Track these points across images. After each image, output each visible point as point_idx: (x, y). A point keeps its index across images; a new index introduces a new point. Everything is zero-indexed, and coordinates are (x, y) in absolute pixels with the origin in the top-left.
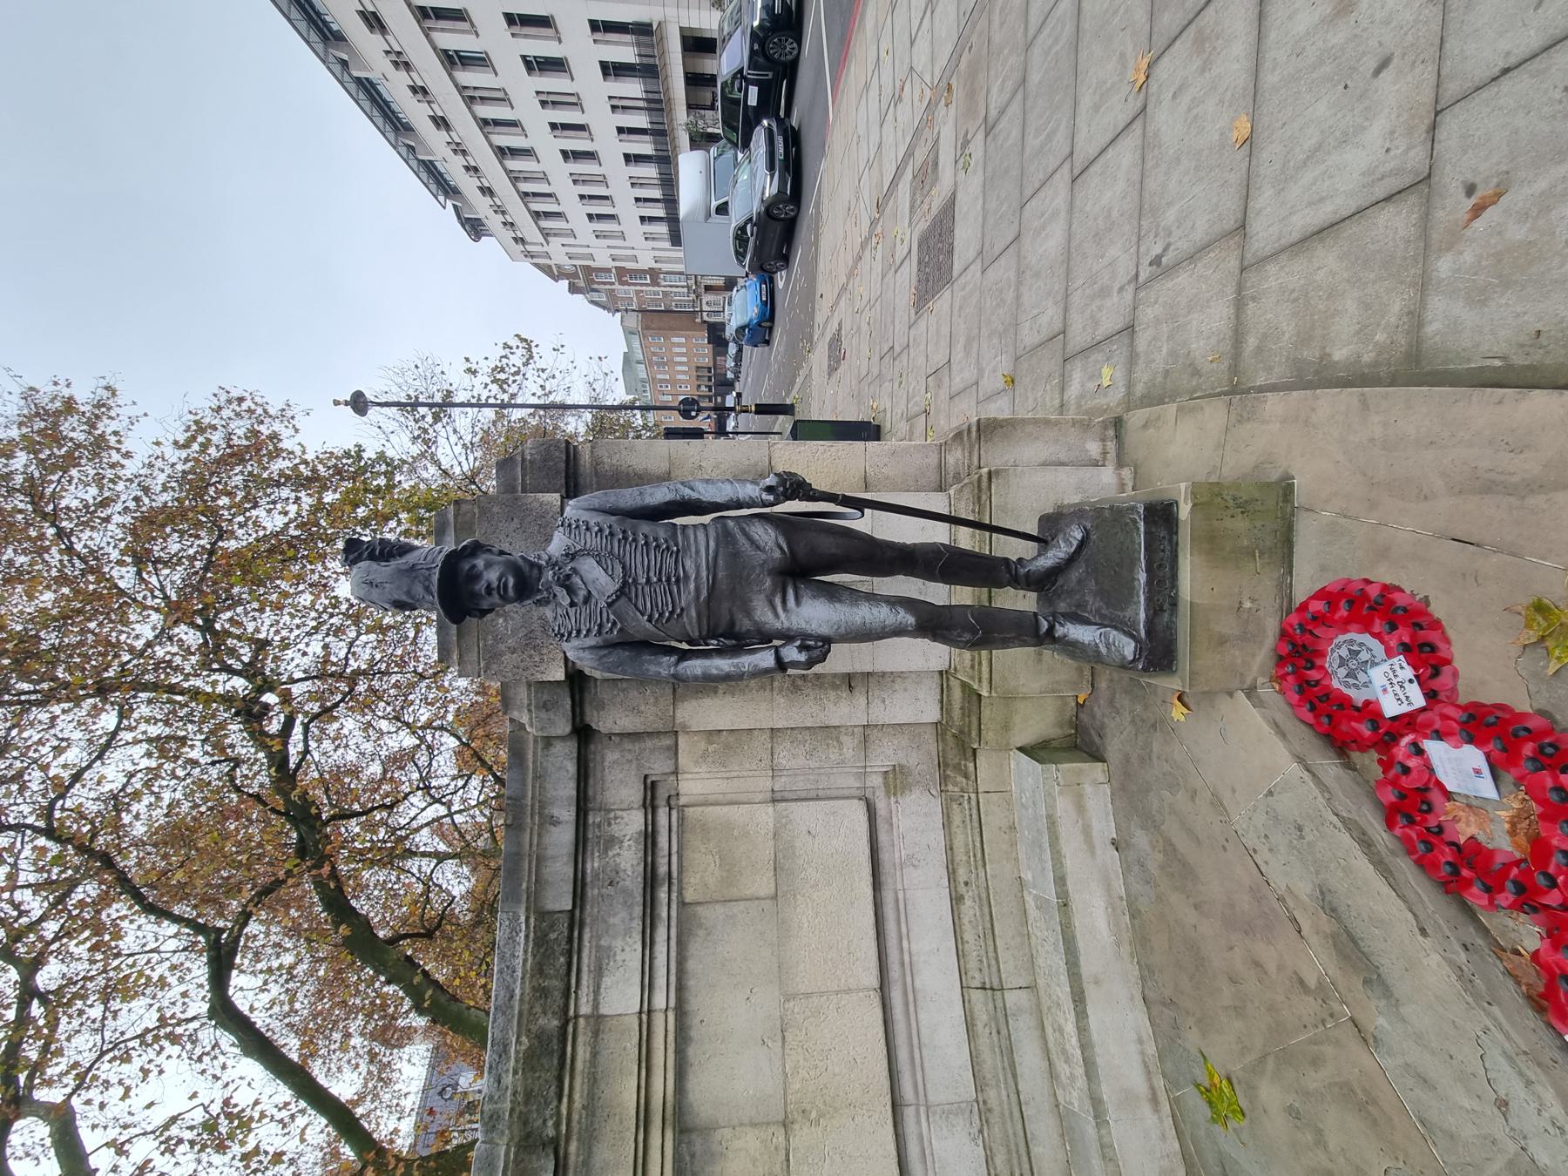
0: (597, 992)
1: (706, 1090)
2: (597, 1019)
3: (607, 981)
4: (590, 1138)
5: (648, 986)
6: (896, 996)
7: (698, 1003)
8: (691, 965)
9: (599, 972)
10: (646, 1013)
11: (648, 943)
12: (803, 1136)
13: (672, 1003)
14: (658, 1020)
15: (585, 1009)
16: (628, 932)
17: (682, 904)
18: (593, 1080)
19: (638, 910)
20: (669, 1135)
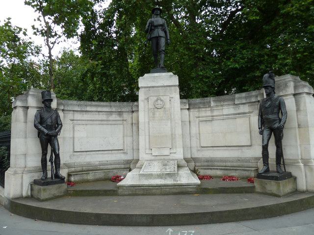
15: (224, 107)
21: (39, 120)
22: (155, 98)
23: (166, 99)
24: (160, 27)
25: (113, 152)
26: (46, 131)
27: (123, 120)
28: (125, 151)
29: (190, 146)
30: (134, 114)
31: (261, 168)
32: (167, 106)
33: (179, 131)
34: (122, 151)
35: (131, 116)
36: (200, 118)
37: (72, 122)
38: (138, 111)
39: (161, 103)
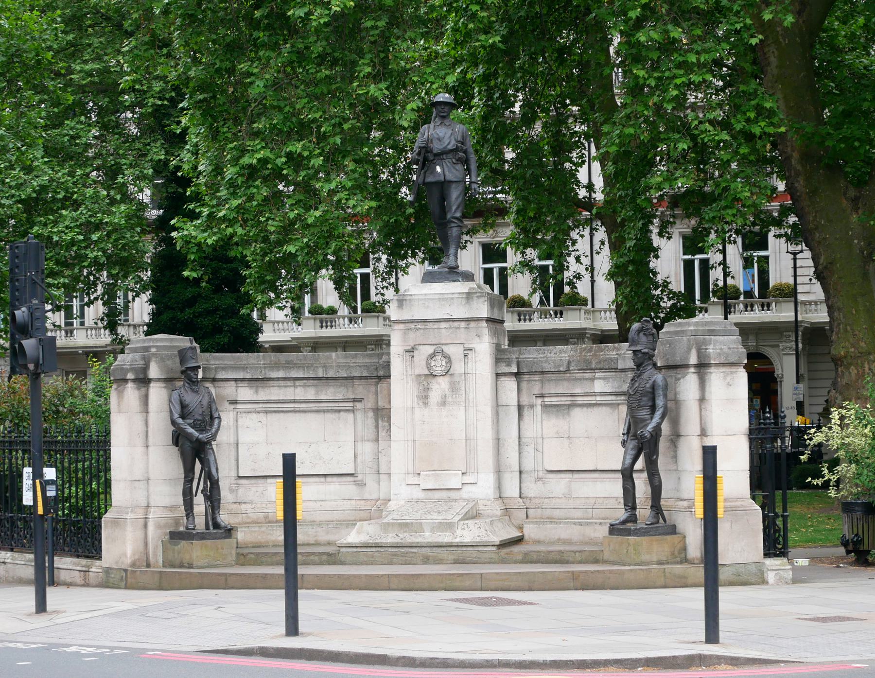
0: (600, 378)
1: (577, 412)
2: (593, 379)
3: (601, 381)
4: (568, 380)
5: (602, 394)
6: (596, 475)
7: (596, 410)
8: (604, 408)
9: (604, 379)
10: (594, 394)
11: (611, 394)
12: (566, 441)
13: (598, 402)
14: (593, 398)
15: (597, 375)
16: (613, 387)
17: (619, 404)
18: (580, 379)
19: (617, 390)
20: (569, 403)
22: (430, 350)
24: (450, 156)
25: (329, 479)
27: (354, 400)
28: (360, 477)
29: (517, 469)
30: (382, 385)
31: (621, 514)
32: (458, 367)
33: (485, 432)
34: (351, 479)
35: (373, 389)
36: (546, 399)
37: (233, 406)
38: (389, 377)
39: (444, 363)
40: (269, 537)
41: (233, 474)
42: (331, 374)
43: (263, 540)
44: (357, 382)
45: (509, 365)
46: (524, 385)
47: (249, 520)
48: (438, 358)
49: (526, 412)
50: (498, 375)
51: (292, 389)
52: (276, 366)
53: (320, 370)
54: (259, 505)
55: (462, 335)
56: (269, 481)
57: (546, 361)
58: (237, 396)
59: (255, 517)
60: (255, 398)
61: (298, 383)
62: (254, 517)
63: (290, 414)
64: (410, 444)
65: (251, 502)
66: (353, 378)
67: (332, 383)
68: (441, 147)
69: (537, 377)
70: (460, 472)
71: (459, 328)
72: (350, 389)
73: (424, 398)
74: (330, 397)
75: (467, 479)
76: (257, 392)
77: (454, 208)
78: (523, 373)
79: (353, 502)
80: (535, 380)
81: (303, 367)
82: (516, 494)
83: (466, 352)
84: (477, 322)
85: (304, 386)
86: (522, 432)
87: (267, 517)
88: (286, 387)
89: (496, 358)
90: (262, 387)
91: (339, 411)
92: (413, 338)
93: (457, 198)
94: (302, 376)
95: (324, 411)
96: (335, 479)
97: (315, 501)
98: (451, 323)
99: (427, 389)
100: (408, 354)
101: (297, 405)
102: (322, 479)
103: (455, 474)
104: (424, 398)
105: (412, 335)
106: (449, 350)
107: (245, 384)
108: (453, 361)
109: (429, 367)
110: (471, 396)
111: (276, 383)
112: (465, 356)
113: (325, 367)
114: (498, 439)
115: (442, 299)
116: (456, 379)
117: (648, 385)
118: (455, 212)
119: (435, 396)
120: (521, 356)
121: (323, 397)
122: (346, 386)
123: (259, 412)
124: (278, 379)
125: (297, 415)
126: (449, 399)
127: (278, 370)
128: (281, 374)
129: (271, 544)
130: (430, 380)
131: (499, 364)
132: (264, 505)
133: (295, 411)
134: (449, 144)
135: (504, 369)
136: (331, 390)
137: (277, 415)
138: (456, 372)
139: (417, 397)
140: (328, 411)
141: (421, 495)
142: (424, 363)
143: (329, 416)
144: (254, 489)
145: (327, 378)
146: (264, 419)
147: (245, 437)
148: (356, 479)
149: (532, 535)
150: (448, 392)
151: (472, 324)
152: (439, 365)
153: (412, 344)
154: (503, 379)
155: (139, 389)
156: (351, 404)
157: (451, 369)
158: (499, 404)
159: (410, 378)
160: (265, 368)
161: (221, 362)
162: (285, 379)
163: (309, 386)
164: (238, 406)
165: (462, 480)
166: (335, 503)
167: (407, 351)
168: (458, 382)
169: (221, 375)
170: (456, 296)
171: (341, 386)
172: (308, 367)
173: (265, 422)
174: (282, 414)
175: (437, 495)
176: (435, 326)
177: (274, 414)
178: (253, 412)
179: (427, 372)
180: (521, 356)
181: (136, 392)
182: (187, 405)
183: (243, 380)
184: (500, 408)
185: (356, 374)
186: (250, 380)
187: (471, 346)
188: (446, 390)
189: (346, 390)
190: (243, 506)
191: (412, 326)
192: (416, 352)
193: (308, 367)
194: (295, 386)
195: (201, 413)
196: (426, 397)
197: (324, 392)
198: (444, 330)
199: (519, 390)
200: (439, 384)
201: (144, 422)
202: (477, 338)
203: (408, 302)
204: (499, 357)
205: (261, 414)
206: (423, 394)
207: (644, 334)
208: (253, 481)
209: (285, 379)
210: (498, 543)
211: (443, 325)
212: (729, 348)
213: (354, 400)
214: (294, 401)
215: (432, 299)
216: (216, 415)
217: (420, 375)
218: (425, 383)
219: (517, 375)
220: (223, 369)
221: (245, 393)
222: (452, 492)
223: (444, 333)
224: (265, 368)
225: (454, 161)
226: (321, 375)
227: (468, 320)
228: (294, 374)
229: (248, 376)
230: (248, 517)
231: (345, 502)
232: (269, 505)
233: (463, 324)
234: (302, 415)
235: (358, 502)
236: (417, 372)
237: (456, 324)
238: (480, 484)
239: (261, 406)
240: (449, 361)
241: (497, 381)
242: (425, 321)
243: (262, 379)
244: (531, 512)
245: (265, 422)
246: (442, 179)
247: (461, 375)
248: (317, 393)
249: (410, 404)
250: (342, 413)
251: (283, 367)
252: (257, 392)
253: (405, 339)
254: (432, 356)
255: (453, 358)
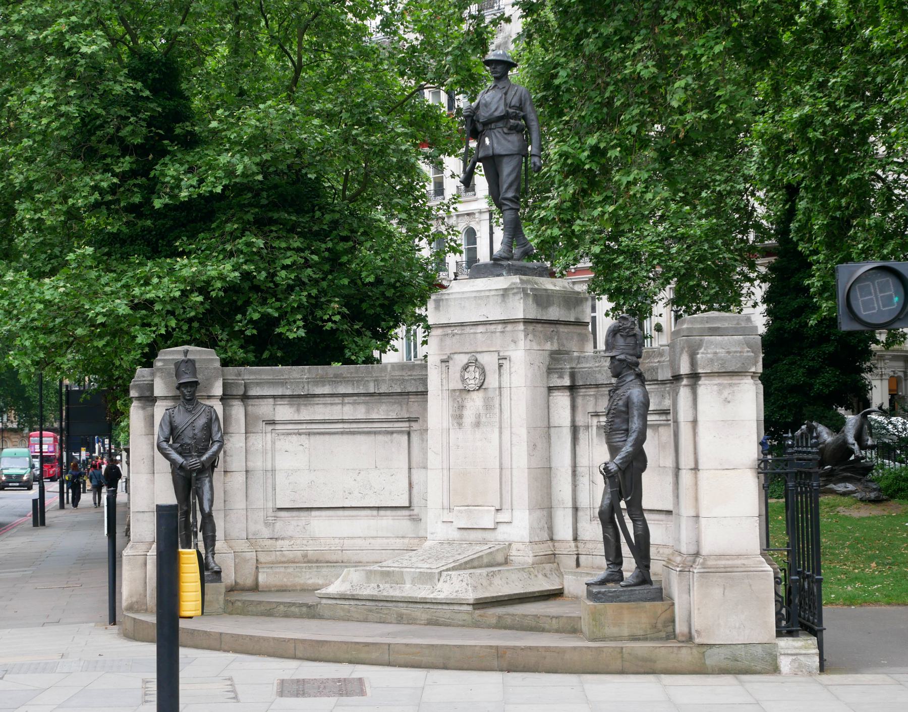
21: (167, 431)
22: (463, 359)
23: (489, 360)
24: (500, 124)
25: (382, 512)
26: (180, 459)
27: (410, 420)
28: (416, 511)
32: (492, 381)
34: (406, 513)
37: (270, 428)
39: (477, 376)
40: (297, 580)
41: (270, 505)
42: (384, 389)
43: (289, 584)
44: (412, 398)
45: (561, 377)
46: (579, 401)
47: (283, 559)
48: (471, 369)
49: (582, 436)
50: (550, 389)
51: (340, 407)
52: (322, 381)
53: (372, 385)
54: (298, 542)
55: (497, 342)
56: (314, 513)
57: (600, 372)
58: (274, 415)
59: (291, 556)
60: (296, 417)
61: (347, 400)
62: (290, 555)
63: (337, 437)
64: (445, 472)
65: (291, 537)
66: (408, 394)
67: (385, 399)
68: (487, 115)
69: (592, 392)
70: (493, 508)
71: (495, 332)
72: (404, 406)
73: (458, 418)
74: (382, 416)
75: (502, 517)
76: (298, 410)
77: (505, 186)
78: (579, 387)
79: (406, 541)
80: (589, 395)
81: (352, 381)
82: (569, 536)
83: (501, 361)
84: (514, 325)
85: (354, 403)
86: (578, 459)
87: (305, 556)
88: (332, 404)
89: (549, 369)
90: (305, 405)
91: (392, 433)
92: (452, 344)
93: (509, 175)
94: (351, 391)
95: (375, 433)
96: (389, 513)
97: (365, 538)
98: (488, 326)
99: (461, 407)
100: (444, 364)
101: (346, 426)
102: (375, 512)
103: (488, 510)
104: (458, 418)
105: (448, 341)
106: (484, 359)
107: (286, 401)
108: (488, 373)
109: (463, 380)
110: (506, 414)
111: (322, 400)
112: (500, 366)
113: (377, 381)
114: (550, 468)
115: (480, 297)
116: (490, 394)
117: (621, 403)
118: (506, 191)
119: (469, 415)
120: (579, 366)
121: (374, 416)
122: (400, 404)
123: (300, 434)
124: (324, 395)
125: (345, 437)
126: (483, 419)
127: (324, 386)
128: (326, 390)
129: (299, 588)
130: (464, 395)
131: (551, 376)
132: (305, 542)
133: (342, 433)
134: (496, 110)
135: (556, 381)
136: (384, 407)
137: (322, 437)
138: (491, 386)
139: (452, 416)
140: (380, 433)
141: (456, 535)
142: (458, 375)
143: (380, 438)
144: (294, 523)
145: (380, 394)
146: (307, 441)
147: (283, 463)
148: (412, 513)
149: (571, 589)
150: (482, 411)
151: (509, 327)
152: (473, 376)
153: (448, 353)
154: (556, 393)
155: (144, 408)
156: (407, 424)
157: (486, 383)
158: (552, 425)
159: (446, 394)
160: (308, 383)
161: (258, 377)
162: (332, 395)
163: (359, 403)
164: (278, 427)
165: (495, 518)
166: (385, 541)
167: (443, 361)
168: (493, 398)
169: (252, 392)
170: (493, 293)
171: (395, 403)
172: (358, 381)
173: (307, 446)
174: (327, 437)
175: (473, 535)
176: (472, 331)
177: (318, 436)
178: (294, 434)
179: (461, 387)
180: (579, 366)
181: (141, 412)
182: (176, 427)
183: (282, 397)
184: (552, 430)
185: (410, 389)
186: (292, 397)
187: (506, 354)
188: (481, 408)
189: (399, 408)
190: (280, 542)
191: (449, 331)
192: (451, 362)
193: (358, 381)
194: (343, 404)
195: (191, 435)
196: (461, 417)
197: (376, 410)
198: (480, 335)
199: (574, 408)
200: (473, 400)
201: (150, 446)
202: (513, 345)
203: (445, 302)
204: (552, 366)
205: (303, 437)
206: (458, 413)
207: (622, 336)
208: (295, 513)
209: (332, 395)
210: (471, 602)
211: (480, 329)
212: (729, 353)
213: (410, 420)
214: (343, 421)
215: (468, 298)
216: (217, 437)
217: (454, 390)
218: (460, 400)
219: (572, 389)
220: (258, 384)
221: (284, 412)
222: (487, 532)
223: (480, 339)
224: (308, 383)
225: (506, 130)
226: (372, 391)
227: (505, 322)
228: (342, 390)
229: (288, 392)
230: (284, 556)
231: (398, 540)
232: (311, 542)
233: (500, 327)
234: (350, 437)
235: (412, 541)
236: (451, 387)
237: (492, 327)
238: (515, 522)
239: (304, 426)
240: (483, 373)
241: (549, 396)
242: (462, 325)
243: (306, 396)
244: (582, 559)
245: (307, 446)
246: (490, 153)
247: (495, 388)
248: (368, 412)
249: (445, 425)
250: (395, 435)
251: (329, 382)
252: (298, 410)
253: (441, 347)
254: (465, 368)
255: (487, 368)
